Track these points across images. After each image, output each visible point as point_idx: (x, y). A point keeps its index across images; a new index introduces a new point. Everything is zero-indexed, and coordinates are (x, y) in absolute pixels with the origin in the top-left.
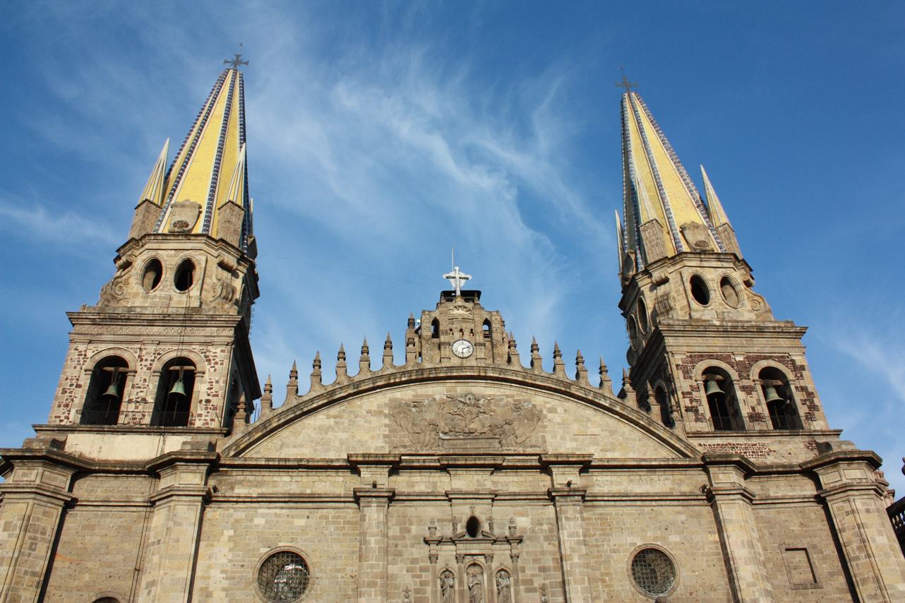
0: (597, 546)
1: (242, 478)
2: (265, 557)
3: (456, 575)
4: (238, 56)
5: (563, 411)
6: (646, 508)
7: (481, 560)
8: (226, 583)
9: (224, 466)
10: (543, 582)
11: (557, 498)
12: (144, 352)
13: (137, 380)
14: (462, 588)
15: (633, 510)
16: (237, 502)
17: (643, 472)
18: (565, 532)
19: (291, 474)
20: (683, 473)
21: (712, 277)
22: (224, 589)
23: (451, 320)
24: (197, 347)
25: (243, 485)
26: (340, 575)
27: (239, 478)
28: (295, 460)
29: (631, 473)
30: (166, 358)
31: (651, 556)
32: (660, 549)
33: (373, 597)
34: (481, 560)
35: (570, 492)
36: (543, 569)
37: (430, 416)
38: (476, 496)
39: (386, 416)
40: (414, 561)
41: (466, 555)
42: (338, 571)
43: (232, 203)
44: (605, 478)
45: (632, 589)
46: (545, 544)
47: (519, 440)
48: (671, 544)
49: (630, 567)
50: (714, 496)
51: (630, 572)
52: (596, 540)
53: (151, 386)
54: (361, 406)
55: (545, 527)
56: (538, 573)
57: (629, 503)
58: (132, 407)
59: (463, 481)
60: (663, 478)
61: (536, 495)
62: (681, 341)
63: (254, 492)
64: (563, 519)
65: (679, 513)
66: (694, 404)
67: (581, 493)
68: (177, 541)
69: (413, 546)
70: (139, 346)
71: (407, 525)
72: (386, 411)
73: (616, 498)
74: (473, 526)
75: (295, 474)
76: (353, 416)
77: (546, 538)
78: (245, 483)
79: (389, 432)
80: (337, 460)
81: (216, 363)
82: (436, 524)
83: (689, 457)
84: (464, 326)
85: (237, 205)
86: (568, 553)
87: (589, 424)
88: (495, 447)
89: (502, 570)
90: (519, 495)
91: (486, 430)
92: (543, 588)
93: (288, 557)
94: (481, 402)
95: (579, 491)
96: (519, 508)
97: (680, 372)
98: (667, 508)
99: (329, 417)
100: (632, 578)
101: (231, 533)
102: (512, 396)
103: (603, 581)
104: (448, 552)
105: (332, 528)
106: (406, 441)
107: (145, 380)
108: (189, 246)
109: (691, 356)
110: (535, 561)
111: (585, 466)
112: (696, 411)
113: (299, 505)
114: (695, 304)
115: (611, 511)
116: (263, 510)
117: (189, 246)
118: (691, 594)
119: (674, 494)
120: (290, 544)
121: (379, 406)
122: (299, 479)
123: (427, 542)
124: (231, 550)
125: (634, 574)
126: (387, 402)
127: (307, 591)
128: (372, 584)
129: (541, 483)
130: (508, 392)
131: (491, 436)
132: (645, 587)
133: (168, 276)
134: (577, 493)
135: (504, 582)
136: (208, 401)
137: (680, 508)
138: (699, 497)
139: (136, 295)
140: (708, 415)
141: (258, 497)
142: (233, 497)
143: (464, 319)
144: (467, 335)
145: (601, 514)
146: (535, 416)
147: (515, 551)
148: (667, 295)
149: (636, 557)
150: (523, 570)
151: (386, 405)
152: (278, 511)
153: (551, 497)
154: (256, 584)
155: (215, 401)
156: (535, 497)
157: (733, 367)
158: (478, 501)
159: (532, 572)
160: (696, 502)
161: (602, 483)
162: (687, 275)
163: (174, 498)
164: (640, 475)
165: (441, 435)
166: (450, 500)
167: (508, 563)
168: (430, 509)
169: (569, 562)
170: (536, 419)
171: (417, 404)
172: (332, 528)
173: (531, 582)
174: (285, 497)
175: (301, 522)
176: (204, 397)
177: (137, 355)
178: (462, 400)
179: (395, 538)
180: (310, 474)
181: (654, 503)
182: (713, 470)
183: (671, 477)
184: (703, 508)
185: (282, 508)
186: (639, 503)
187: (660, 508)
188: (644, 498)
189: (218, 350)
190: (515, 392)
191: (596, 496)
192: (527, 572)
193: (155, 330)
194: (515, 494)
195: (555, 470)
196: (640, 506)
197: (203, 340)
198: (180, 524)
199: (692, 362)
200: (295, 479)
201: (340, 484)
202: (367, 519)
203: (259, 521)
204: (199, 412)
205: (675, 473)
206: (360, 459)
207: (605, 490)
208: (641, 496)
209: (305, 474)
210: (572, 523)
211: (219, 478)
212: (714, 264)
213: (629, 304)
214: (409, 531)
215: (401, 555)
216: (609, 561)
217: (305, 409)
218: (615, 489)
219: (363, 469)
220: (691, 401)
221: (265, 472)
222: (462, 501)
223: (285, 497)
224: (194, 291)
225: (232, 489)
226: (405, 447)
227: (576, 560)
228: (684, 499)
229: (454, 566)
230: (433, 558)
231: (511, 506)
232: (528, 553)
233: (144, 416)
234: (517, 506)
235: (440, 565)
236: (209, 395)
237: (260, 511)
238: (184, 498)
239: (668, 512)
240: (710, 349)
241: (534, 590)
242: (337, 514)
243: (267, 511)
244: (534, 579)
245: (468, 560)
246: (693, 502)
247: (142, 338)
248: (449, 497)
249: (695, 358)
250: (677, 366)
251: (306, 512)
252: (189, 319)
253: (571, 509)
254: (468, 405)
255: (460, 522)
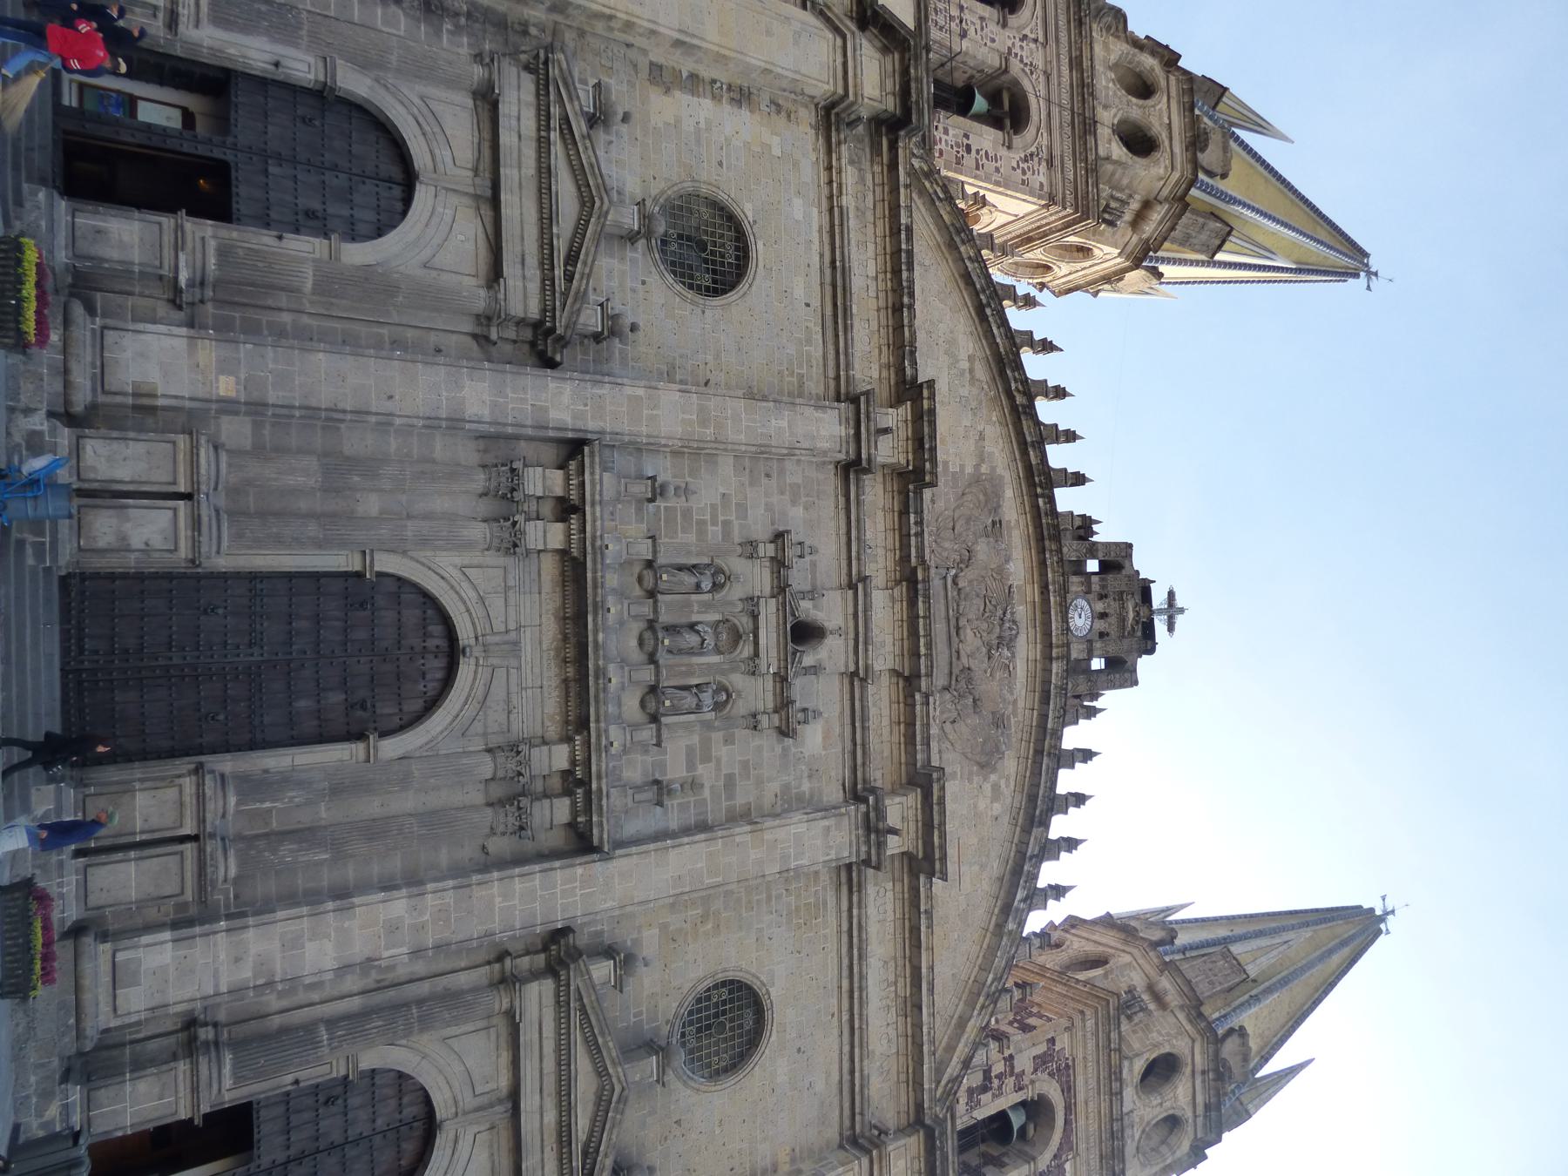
0: (769, 898)
1: (869, 182)
2: (738, 212)
3: (717, 596)
4: (1376, 274)
5: (995, 813)
6: (835, 1001)
7: (746, 650)
8: (688, 126)
9: (893, 147)
10: (707, 785)
11: (863, 808)
12: (1033, 46)
13: (993, 28)
14: (696, 608)
15: (832, 972)
16: (829, 168)
17: (904, 989)
18: (802, 828)
19: (881, 276)
20: (903, 1077)
21: (1181, 1095)
22: (678, 121)
23: (1120, 596)
24: (1045, 142)
25: (858, 183)
26: (709, 358)
27: (869, 177)
28: (911, 282)
29: (900, 962)
30: (1026, 84)
31: (749, 1022)
32: (764, 1041)
33: (681, 416)
34: (746, 650)
35: (874, 829)
36: (730, 782)
37: (982, 549)
38: (860, 639)
39: (977, 467)
40: (742, 510)
41: (755, 617)
42: (717, 356)
43: (1229, 234)
44: (889, 907)
45: (688, 986)
46: (774, 787)
47: (948, 726)
48: (773, 1063)
49: (731, 975)
50: (869, 1152)
51: (720, 977)
52: (779, 897)
53: (985, 50)
54: (989, 422)
55: (806, 786)
56: (724, 772)
57: (846, 962)
58: (955, 12)
59: (885, 611)
60: (893, 1034)
61: (864, 764)
62: (1091, 1045)
63: (848, 201)
64: (826, 823)
65: (828, 1074)
66: (996, 1082)
67: (874, 858)
68: (769, 33)
69: (769, 508)
70: (1041, 39)
71: (804, 499)
72: (984, 469)
73: (855, 933)
74: (804, 633)
75: (881, 286)
76: (974, 405)
77: (786, 788)
78: (860, 187)
79: (954, 474)
80: (914, 363)
81: (1024, 173)
82: (808, 558)
83: (938, 1082)
84: (1113, 620)
85: (1223, 242)
86: (768, 836)
87: (976, 868)
88: (940, 679)
89: (729, 696)
90: (863, 728)
91: (964, 660)
92: (694, 785)
93: (737, 258)
94: (1006, 653)
95: (879, 855)
96: (837, 730)
97: (1041, 1049)
98: (836, 1047)
99: (971, 359)
100: (709, 983)
101: (777, 152)
102: (1015, 713)
103: (704, 918)
104: (758, 578)
105: (791, 350)
106: (941, 504)
107: (993, 41)
108: (1177, 150)
109: (1067, 1066)
110: (745, 765)
111: (925, 863)
112: (984, 1089)
113: (828, 289)
114: (1139, 1065)
115: (830, 925)
116: (816, 218)
117: (1177, 150)
118: (678, 1122)
119: (866, 1062)
120: (761, 265)
121: (991, 454)
122: (872, 293)
123: (779, 537)
124: (747, 144)
125: (716, 987)
126: (1000, 471)
127: (679, 287)
128: (704, 422)
129: (882, 768)
130: (1021, 704)
131: (956, 671)
132: (691, 1013)
133: (1134, 109)
134: (873, 852)
135: (707, 698)
136: (968, 149)
137: (837, 1078)
138: (858, 1118)
139: (1106, 46)
140: (981, 1114)
141: (841, 208)
142: (839, 159)
143: (1122, 620)
144: (1100, 625)
145: (825, 903)
146: (986, 762)
147: (764, 721)
148: (1150, 1013)
149: (749, 988)
150: (728, 741)
151: (993, 469)
152: (816, 246)
153: (858, 793)
154: (688, 186)
155: (969, 161)
156: (859, 761)
157: (1055, 1157)
158: (851, 643)
159: (724, 759)
160: (847, 1112)
161: (882, 900)
162: (1180, 1046)
163: (839, 41)
164: (895, 983)
165: (953, 572)
166: (852, 586)
167: (740, 708)
168: (834, 548)
169: (748, 837)
170: (983, 759)
171: (997, 524)
172: (791, 350)
173: (706, 758)
174: (843, 260)
175: (799, 292)
176: (974, 142)
177: (1027, 31)
178: (1008, 616)
179: (782, 472)
180: (883, 313)
181: (845, 1017)
182: (915, 1143)
183: (894, 1050)
184: (836, 1128)
185: (822, 256)
186: (845, 984)
187: (836, 1032)
188: (856, 995)
189: (1042, 179)
190: (1020, 718)
191: (859, 891)
192: (722, 751)
193: (1065, 70)
194: (864, 719)
195: (913, 799)
196: (840, 987)
197: (1057, 152)
198: (796, 43)
199: (1059, 1070)
200: (872, 285)
201: (869, 368)
202: (819, 414)
203: (798, 209)
204: (951, 132)
205: (902, 1059)
206: (926, 403)
207: (871, 911)
208: (861, 989)
209: (882, 303)
210: (819, 842)
211: (867, 140)
212: (1200, 1099)
213: (1085, 935)
214: (794, 502)
215: (751, 484)
216: (740, 928)
217: (988, 311)
218: (873, 929)
219: (905, 411)
220: (1000, 1076)
221: (882, 227)
222: (851, 610)
223: (843, 260)
224: (1118, 151)
225: (851, 162)
226: (933, 501)
227: (754, 854)
228: (852, 1087)
229: (735, 592)
230: (750, 549)
231: (842, 713)
232: (759, 749)
233: (941, 29)
234: (842, 725)
235: (736, 564)
236: (978, 152)
237: (815, 211)
238: (839, 60)
239: (828, 1047)
240: (1080, 1107)
241: (691, 766)
242: (814, 363)
243: (815, 227)
244: (712, 765)
245: (744, 622)
246: (847, 1105)
247: (1052, 42)
248: (855, 583)
249: (1065, 1075)
250: (1052, 1041)
251: (816, 303)
252: (1085, 127)
253: (834, 839)
254: (1001, 626)
255: (815, 607)
